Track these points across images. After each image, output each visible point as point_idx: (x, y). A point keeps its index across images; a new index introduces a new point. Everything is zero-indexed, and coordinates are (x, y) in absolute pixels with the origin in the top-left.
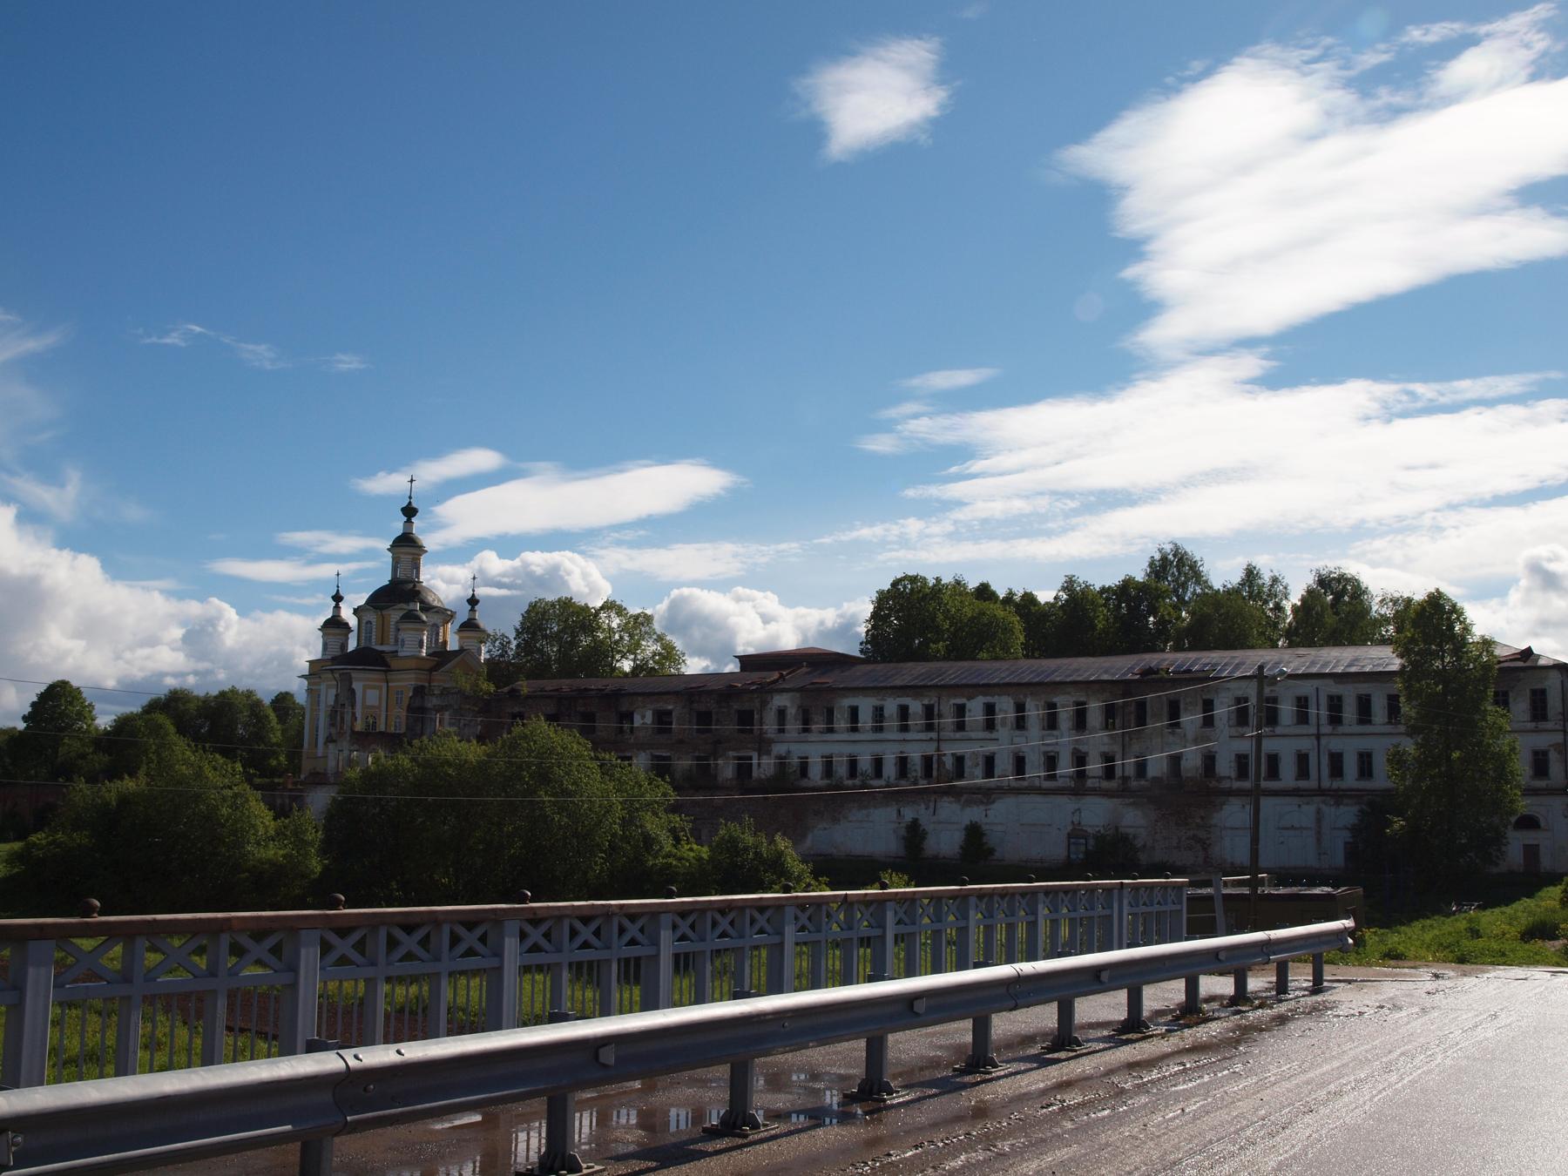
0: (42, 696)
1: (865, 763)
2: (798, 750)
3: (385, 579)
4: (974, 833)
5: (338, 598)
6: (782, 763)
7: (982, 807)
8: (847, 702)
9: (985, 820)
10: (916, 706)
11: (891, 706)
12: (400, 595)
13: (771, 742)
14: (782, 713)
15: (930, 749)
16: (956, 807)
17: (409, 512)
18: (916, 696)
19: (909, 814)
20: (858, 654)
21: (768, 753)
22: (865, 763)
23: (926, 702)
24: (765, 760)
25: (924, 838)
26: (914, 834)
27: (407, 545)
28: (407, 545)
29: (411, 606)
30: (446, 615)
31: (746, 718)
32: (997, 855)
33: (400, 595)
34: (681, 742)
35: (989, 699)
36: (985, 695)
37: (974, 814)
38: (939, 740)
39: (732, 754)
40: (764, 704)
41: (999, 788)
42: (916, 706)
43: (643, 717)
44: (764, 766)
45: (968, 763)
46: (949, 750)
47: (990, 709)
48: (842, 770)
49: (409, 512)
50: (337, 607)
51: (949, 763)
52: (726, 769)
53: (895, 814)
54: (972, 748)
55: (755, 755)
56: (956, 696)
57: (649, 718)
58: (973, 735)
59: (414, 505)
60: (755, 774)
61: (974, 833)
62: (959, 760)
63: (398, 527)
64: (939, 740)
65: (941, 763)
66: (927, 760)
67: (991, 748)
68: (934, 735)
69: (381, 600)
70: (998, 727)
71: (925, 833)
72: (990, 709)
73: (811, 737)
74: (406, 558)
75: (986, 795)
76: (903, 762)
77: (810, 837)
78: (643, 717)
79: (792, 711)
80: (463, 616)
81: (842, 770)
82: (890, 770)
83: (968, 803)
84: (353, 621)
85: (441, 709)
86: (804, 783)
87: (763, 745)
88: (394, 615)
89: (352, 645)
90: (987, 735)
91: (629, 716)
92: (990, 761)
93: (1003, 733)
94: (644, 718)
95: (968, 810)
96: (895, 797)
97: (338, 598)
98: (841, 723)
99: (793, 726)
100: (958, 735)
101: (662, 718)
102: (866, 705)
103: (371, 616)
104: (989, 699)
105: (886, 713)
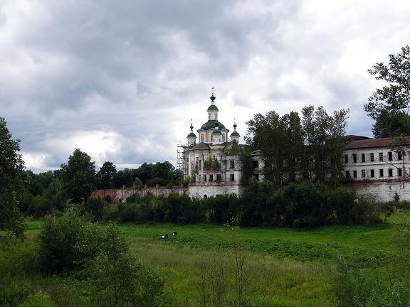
3: (206, 120)
5: (192, 127)
12: (213, 126)
15: (401, 166)
17: (213, 98)
20: (371, 136)
27: (213, 109)
28: (213, 109)
33: (213, 126)
49: (213, 98)
63: (209, 103)
68: (402, 161)
69: (206, 128)
73: (357, 164)
80: (232, 131)
84: (197, 135)
86: (355, 179)
89: (197, 142)
96: (389, 182)
97: (192, 127)
102: (376, 153)
103: (204, 133)
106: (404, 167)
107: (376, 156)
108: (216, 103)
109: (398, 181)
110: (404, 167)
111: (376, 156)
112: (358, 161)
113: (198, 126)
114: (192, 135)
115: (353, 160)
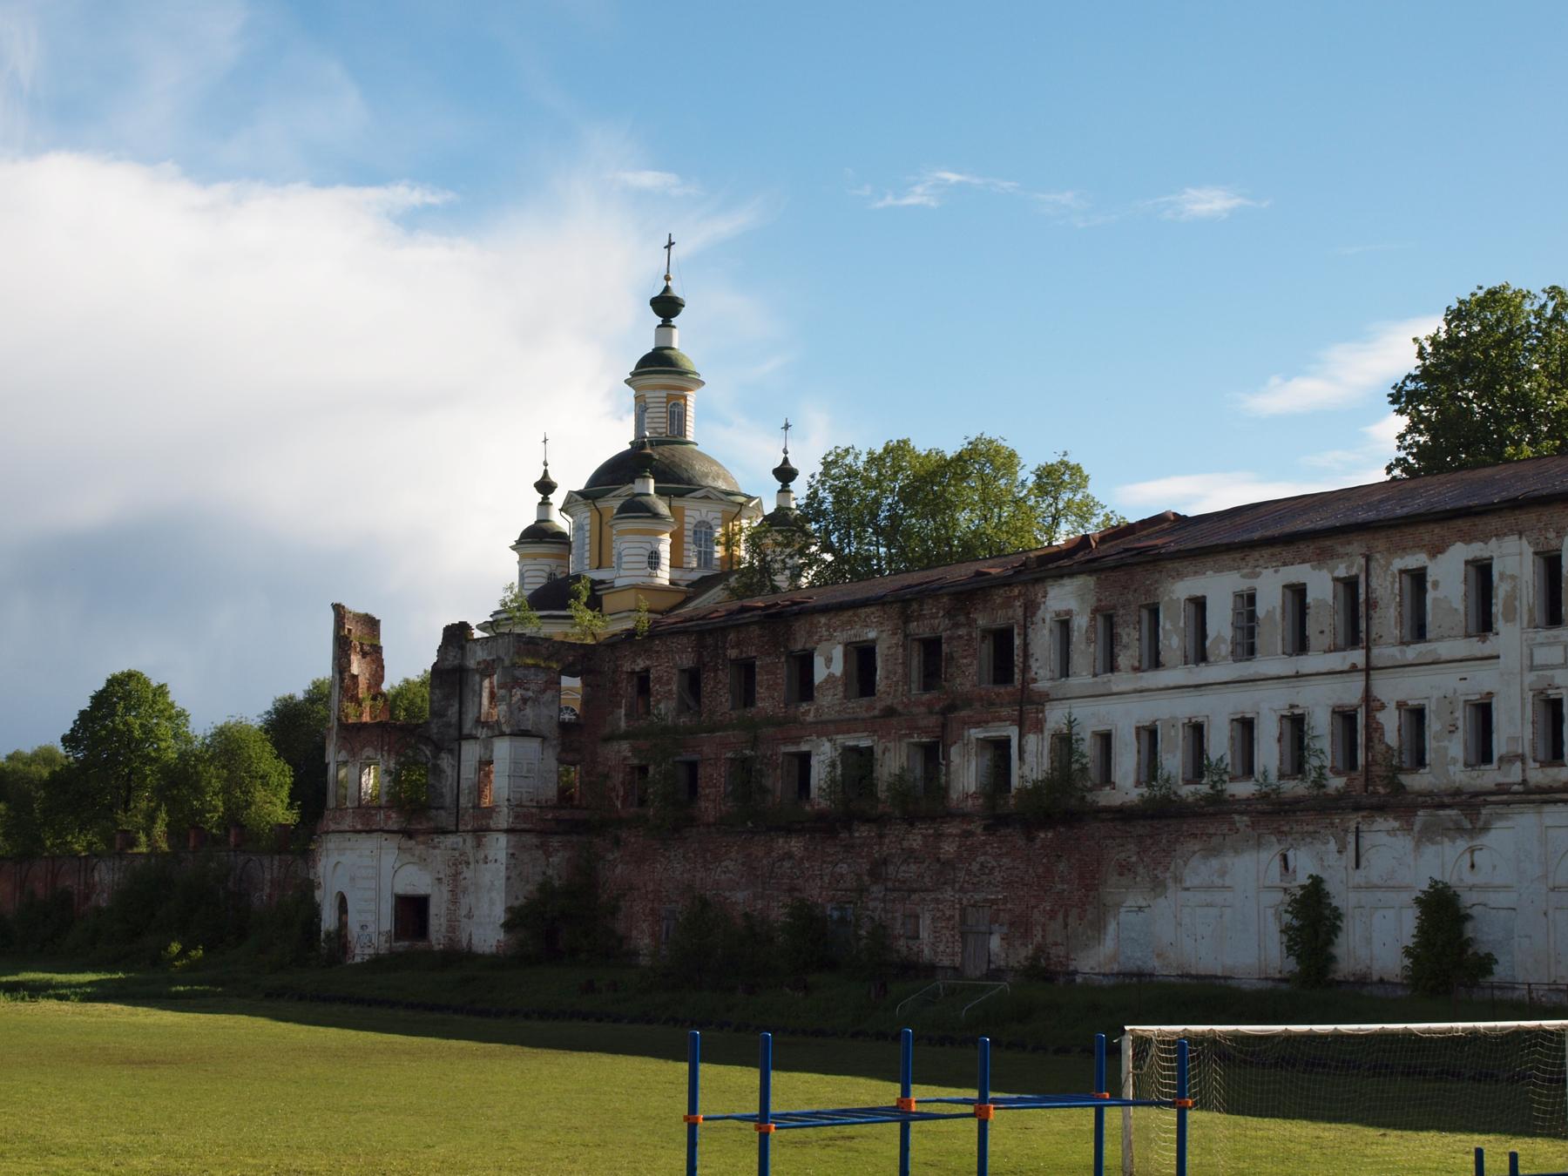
0: (100, 699)
1: (1219, 745)
2: (1089, 717)
3: (619, 438)
4: (1442, 911)
6: (1065, 742)
7: (1462, 844)
8: (1182, 589)
9: (1469, 878)
10: (1321, 585)
11: (1270, 586)
13: (1043, 699)
14: (1064, 625)
15: (1350, 692)
16: (1404, 843)
17: (666, 306)
18: (1322, 558)
19: (1305, 864)
21: (1039, 727)
22: (1219, 745)
23: (1342, 572)
24: (1032, 740)
25: (1335, 930)
26: (1313, 920)
28: (659, 368)
29: (638, 487)
30: (733, 503)
31: (1004, 653)
32: (1501, 972)
33: (654, 470)
34: (890, 712)
35: (1476, 550)
36: (1468, 538)
37: (1441, 861)
38: (1369, 669)
39: (976, 733)
40: (1031, 608)
41: (1502, 789)
42: (1321, 585)
43: (829, 661)
44: (1032, 763)
45: (1433, 725)
46: (1393, 689)
47: (1482, 573)
48: (1173, 761)
49: (666, 306)
50: (545, 504)
51: (1390, 722)
52: (966, 774)
53: (1277, 864)
54: (1432, 679)
55: (1013, 732)
56: (1404, 550)
57: (838, 668)
58: (1445, 649)
59: (676, 291)
60: (1015, 781)
61: (1442, 911)
62: (1417, 715)
64: (1369, 669)
65: (1373, 728)
66: (1345, 718)
67: (1482, 680)
68: (1357, 657)
70: (1499, 624)
71: (1338, 914)
72: (1482, 573)
73: (1122, 681)
74: (656, 397)
75: (1469, 810)
76: (1296, 723)
77: (1112, 928)
78: (829, 661)
79: (1081, 622)
81: (1173, 761)
82: (1269, 753)
83: (1429, 834)
85: (487, 670)
86: (1107, 798)
87: (1028, 708)
88: (612, 504)
90: (1474, 647)
91: (805, 663)
92: (1483, 712)
93: (1509, 637)
94: (829, 665)
95: (1430, 851)
96: (1276, 815)
98: (1173, 639)
99: (1084, 654)
100: (1413, 652)
101: (862, 658)
102: (1218, 588)
103: (586, 515)
104: (1476, 550)
105: (1261, 610)
106: (1368, 697)
107: (1220, 623)
108: (681, 340)
109: (1322, 809)
110: (1370, 700)
111: (1220, 623)
112: (1123, 660)
113: (573, 477)
114: (537, 536)
115: (1097, 650)
